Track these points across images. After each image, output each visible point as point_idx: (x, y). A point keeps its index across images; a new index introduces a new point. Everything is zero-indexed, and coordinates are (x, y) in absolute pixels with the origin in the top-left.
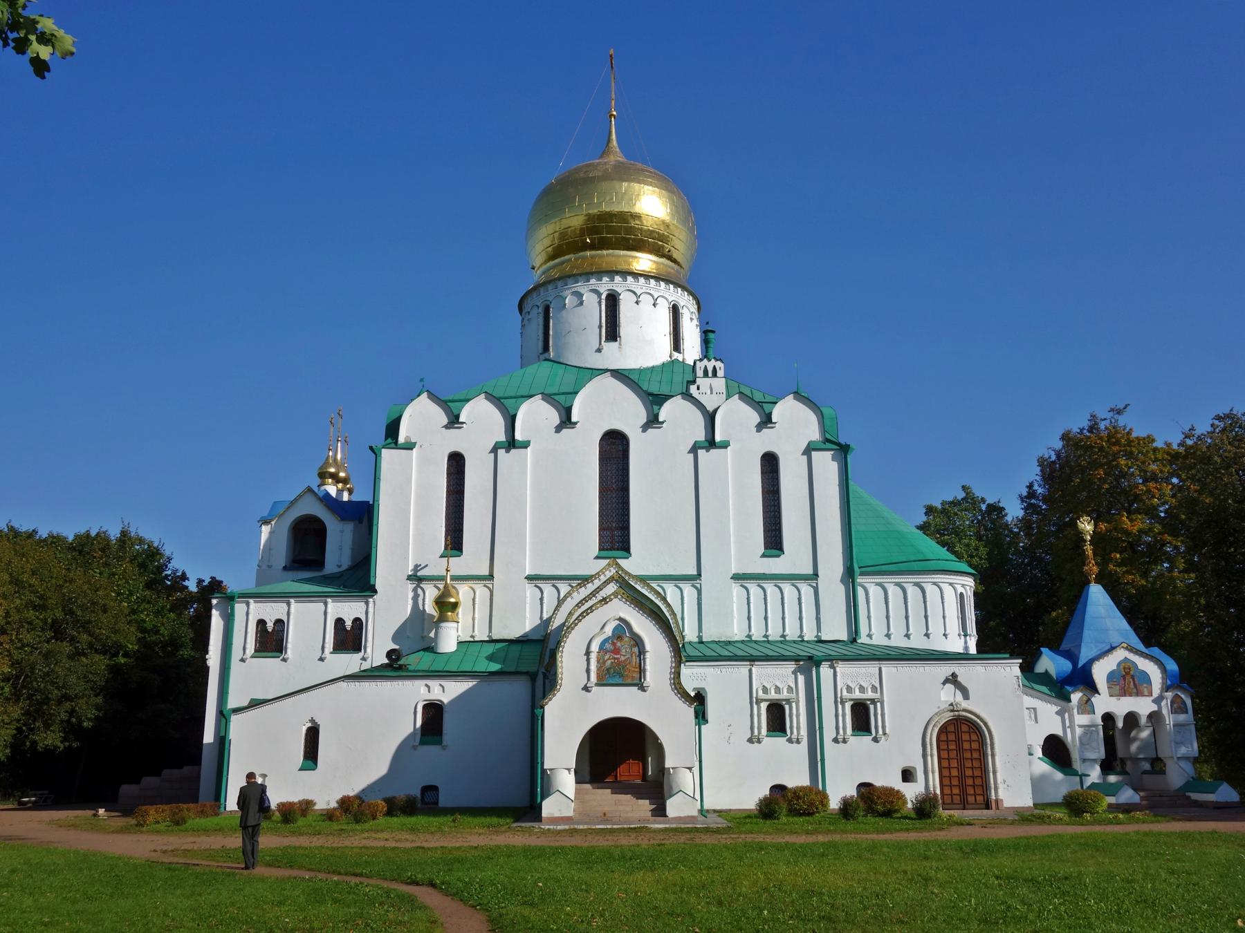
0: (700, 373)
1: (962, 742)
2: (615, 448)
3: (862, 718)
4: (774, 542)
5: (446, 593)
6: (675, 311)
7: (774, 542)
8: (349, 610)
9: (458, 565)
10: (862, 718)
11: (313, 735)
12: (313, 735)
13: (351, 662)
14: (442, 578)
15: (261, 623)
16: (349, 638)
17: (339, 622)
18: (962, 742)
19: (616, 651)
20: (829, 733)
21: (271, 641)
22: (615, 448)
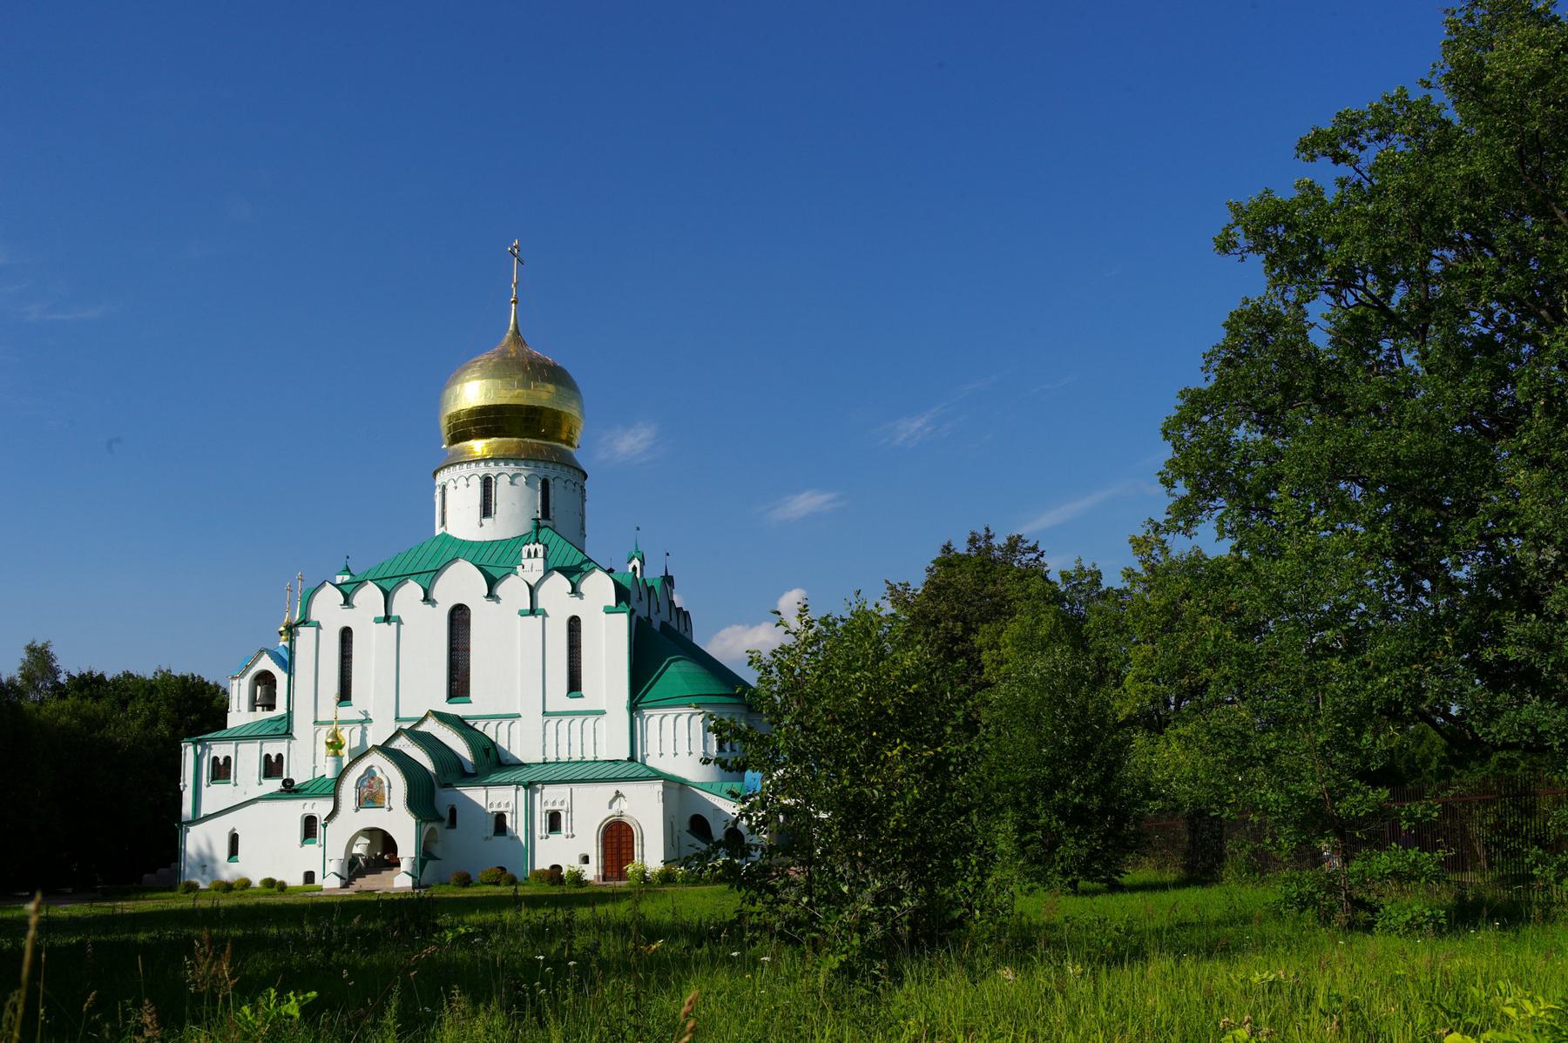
0: (525, 555)
1: (617, 838)
2: (459, 618)
3: (554, 822)
4: (574, 685)
5: (335, 735)
6: (545, 484)
7: (574, 685)
8: (273, 748)
9: (345, 713)
10: (554, 822)
11: (234, 840)
12: (234, 840)
13: (275, 785)
14: (331, 723)
15: (216, 759)
16: (272, 767)
17: (268, 757)
18: (617, 838)
19: (371, 786)
20: (538, 833)
21: (221, 771)
22: (459, 618)
